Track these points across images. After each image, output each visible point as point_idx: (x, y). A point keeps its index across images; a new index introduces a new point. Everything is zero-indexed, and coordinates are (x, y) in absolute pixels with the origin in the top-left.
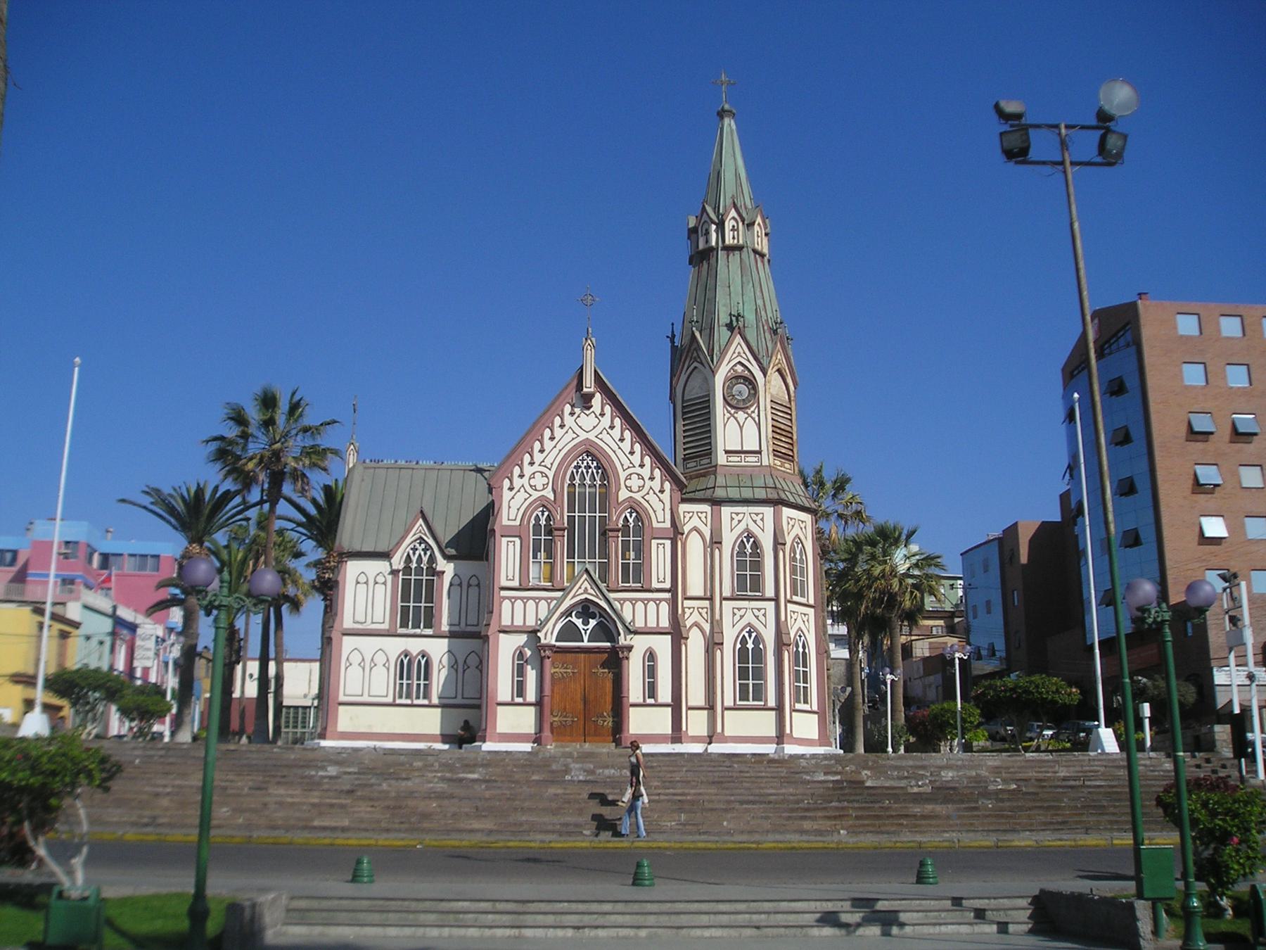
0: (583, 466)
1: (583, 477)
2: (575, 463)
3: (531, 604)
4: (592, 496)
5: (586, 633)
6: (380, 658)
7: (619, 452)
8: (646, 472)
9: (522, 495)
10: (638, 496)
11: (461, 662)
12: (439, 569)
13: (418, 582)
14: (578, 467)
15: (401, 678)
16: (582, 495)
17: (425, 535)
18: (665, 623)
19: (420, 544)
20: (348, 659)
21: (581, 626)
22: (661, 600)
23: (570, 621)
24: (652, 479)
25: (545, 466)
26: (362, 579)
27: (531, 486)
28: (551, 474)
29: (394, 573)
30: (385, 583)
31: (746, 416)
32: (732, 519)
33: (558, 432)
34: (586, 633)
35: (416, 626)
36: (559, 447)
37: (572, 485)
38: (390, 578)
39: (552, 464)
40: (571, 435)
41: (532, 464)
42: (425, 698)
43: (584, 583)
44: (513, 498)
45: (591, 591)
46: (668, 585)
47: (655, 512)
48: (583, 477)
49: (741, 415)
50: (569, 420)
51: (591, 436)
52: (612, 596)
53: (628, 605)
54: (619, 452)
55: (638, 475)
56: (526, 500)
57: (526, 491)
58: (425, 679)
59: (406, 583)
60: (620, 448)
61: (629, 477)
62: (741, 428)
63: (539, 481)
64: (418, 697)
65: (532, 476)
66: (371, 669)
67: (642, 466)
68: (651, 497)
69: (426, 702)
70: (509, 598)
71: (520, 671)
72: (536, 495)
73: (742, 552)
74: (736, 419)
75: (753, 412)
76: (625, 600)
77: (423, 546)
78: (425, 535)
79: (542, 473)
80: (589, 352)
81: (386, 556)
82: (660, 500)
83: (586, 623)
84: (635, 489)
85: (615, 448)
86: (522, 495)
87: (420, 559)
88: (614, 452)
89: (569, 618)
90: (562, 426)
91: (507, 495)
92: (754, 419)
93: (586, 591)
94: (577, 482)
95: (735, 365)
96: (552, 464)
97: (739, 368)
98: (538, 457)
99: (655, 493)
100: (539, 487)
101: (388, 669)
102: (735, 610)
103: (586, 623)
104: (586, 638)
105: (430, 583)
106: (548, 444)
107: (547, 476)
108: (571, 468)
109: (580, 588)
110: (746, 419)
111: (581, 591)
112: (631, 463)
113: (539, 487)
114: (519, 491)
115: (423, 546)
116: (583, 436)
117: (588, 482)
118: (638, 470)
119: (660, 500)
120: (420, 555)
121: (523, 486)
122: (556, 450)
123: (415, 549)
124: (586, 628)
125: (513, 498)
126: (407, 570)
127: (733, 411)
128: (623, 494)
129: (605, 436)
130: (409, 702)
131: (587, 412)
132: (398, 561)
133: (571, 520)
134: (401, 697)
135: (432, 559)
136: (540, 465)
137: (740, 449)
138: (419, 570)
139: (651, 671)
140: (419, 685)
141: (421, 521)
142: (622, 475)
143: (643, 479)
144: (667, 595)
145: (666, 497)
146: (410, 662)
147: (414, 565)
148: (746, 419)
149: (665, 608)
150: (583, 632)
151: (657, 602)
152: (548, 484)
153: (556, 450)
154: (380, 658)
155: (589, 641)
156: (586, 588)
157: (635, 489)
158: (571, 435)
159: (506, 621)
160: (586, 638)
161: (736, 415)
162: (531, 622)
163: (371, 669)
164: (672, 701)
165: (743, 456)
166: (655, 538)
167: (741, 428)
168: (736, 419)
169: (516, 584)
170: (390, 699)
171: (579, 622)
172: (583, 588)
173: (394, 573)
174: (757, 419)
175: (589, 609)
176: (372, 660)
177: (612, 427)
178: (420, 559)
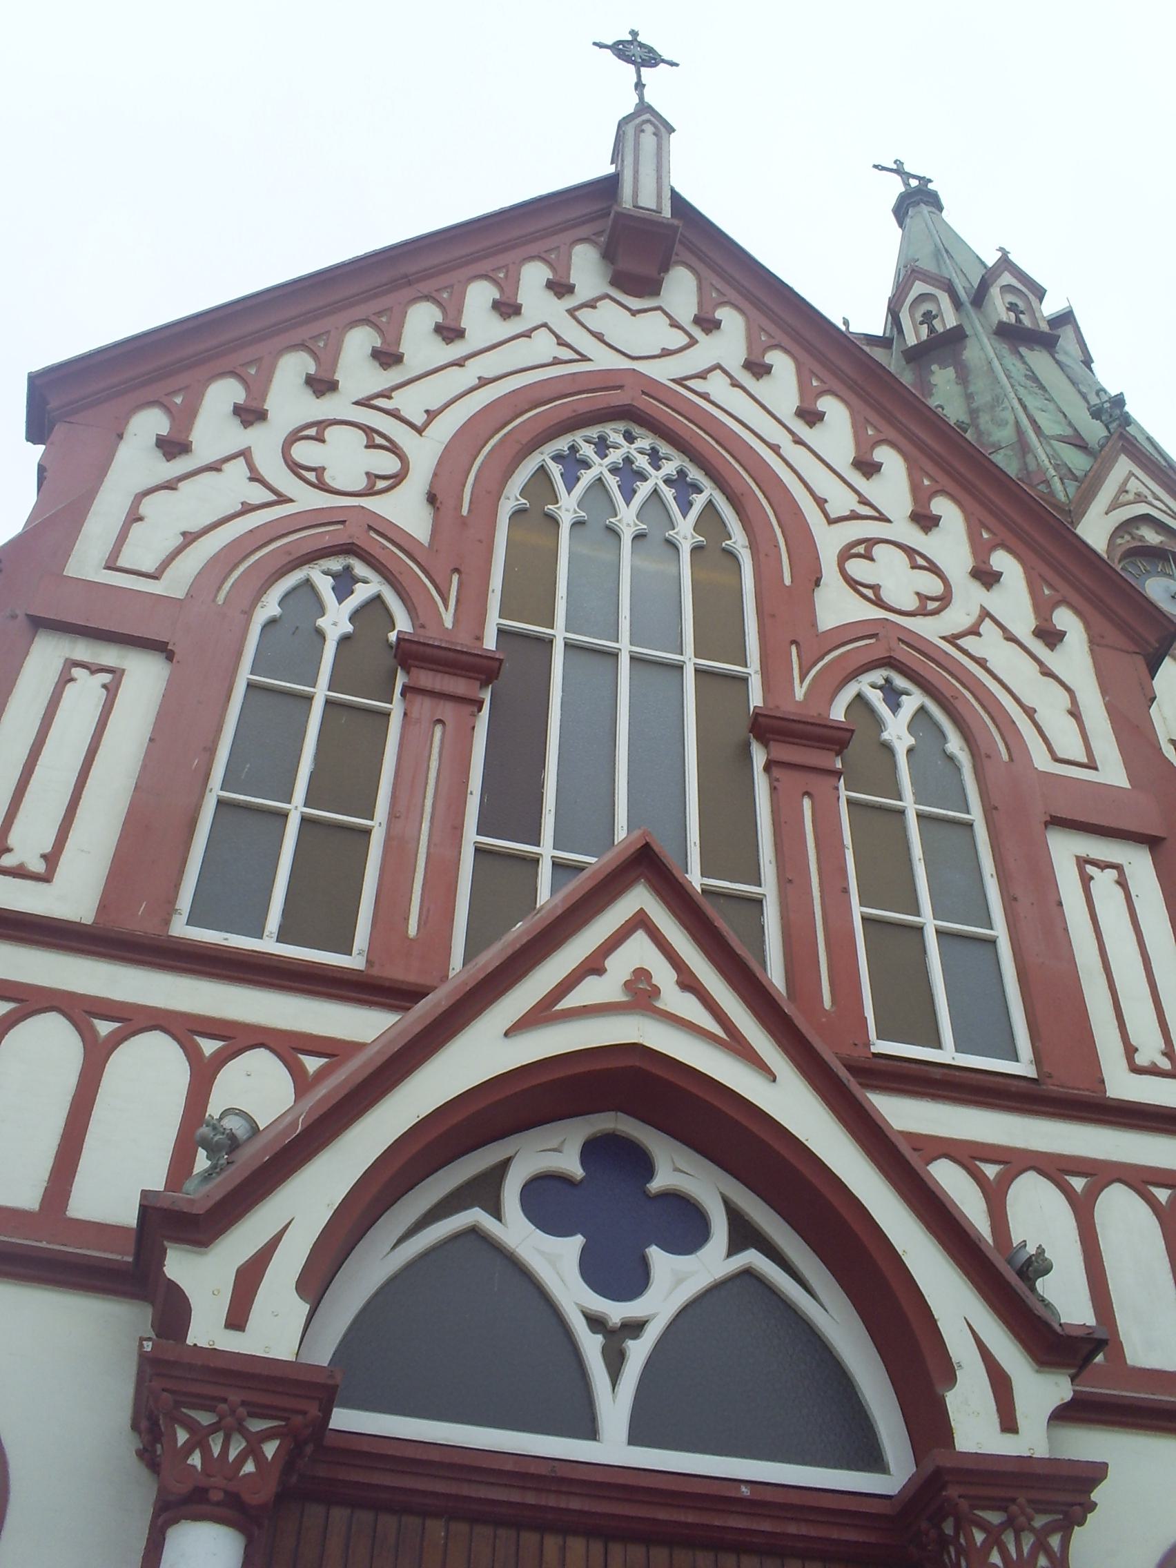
0: (626, 448)
5: (615, 1361)
23: (474, 1231)
25: (395, 414)
34: (615, 1361)
45: (675, 1000)
47: (1030, 712)
56: (247, 509)
60: (798, 441)
61: (865, 549)
79: (368, 431)
82: (1047, 673)
88: (775, 449)
89: (475, 1216)
99: (1010, 638)
109: (593, 966)
112: (864, 501)
114: (215, 467)
124: (616, 1312)
125: (170, 486)
136: (364, 403)
150: (591, 1345)
155: (636, 1437)
172: (620, 965)
175: (646, 1167)
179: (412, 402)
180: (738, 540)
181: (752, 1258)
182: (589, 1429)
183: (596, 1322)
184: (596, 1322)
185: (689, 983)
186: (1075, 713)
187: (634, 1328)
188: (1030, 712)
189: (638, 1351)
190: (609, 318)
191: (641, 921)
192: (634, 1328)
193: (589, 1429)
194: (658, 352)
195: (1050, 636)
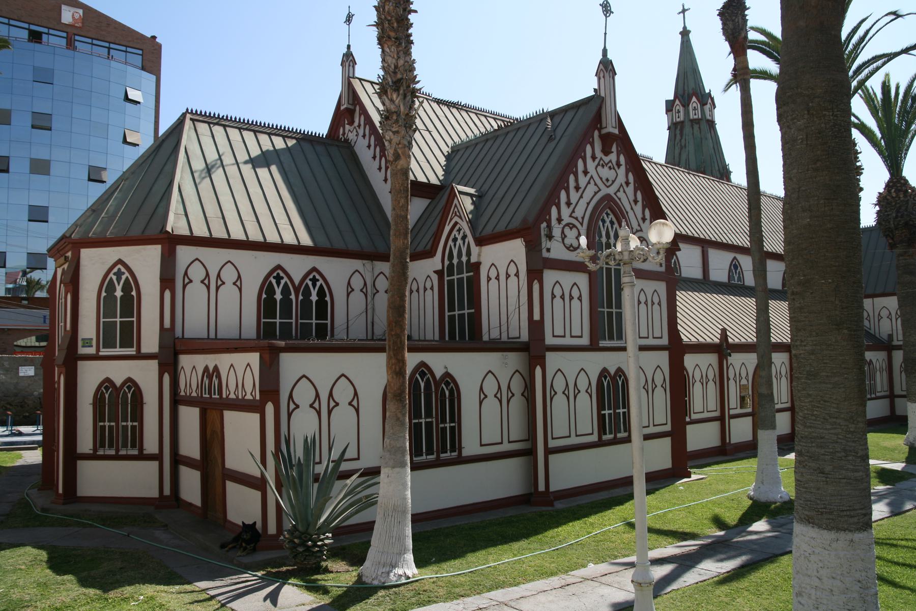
25: (576, 219)
33: (583, 180)
50: (591, 165)
51: (611, 191)
90: (586, 172)
116: (605, 191)
129: (621, 194)
131: (606, 159)
177: (627, 183)
179: (579, 213)
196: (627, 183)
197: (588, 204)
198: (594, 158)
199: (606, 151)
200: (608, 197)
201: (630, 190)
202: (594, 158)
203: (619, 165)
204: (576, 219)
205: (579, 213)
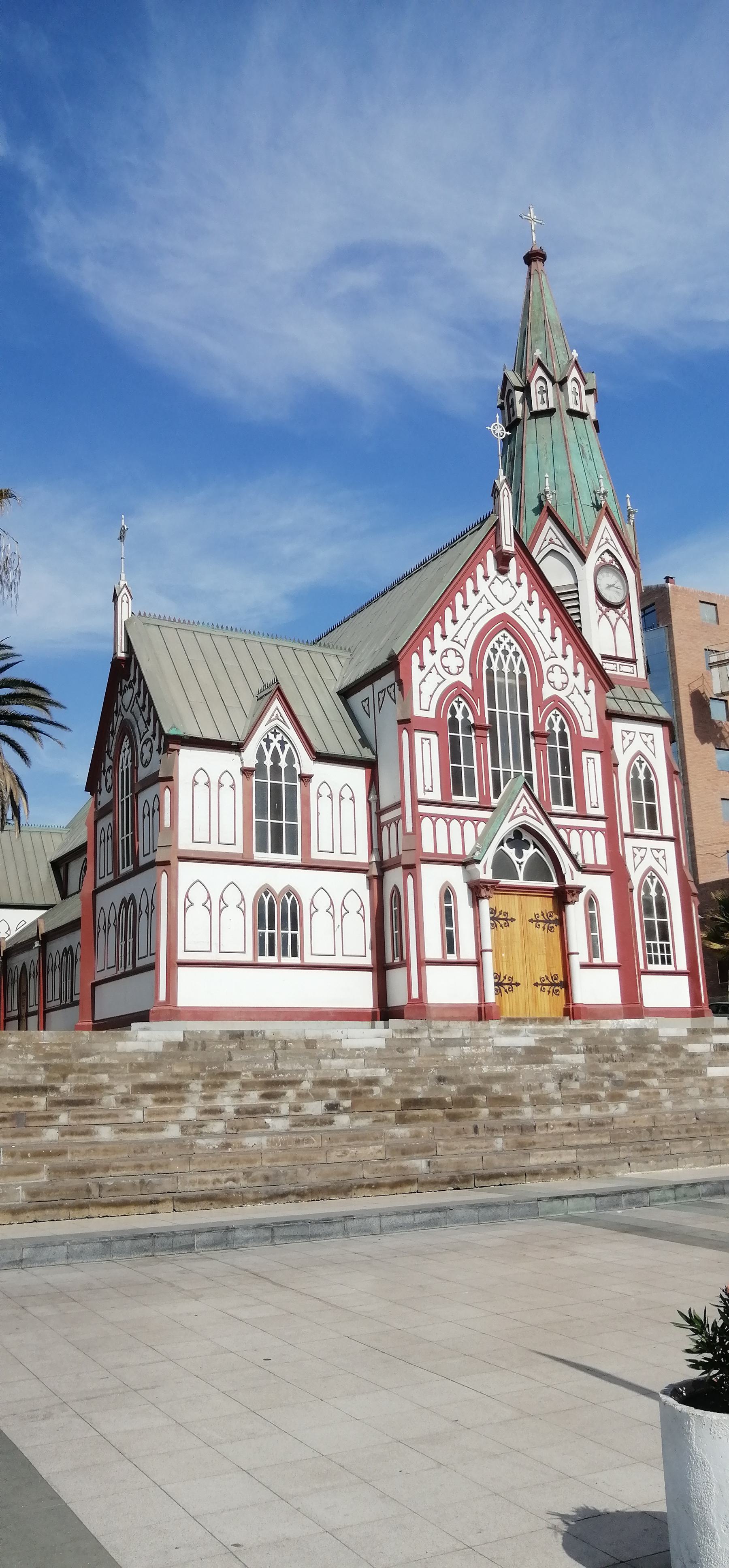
1: (500, 664)
2: (490, 646)
3: (469, 825)
4: (512, 687)
5: (520, 867)
6: (233, 898)
7: (538, 635)
8: (568, 664)
9: (433, 679)
10: (562, 695)
11: (338, 906)
12: (305, 772)
13: (276, 789)
14: (494, 651)
15: (262, 926)
16: (502, 686)
17: (284, 722)
18: (603, 860)
19: (275, 734)
20: (187, 896)
21: (515, 859)
22: (597, 830)
23: (501, 849)
24: (576, 674)
25: (458, 642)
26: (201, 778)
27: (444, 667)
28: (467, 654)
29: (246, 772)
30: (233, 786)
31: (617, 616)
32: (623, 738)
33: (472, 599)
34: (520, 867)
35: (277, 849)
36: (474, 618)
37: (490, 673)
38: (239, 778)
39: (466, 641)
40: (484, 606)
41: (444, 636)
42: (294, 954)
43: (523, 802)
44: (424, 680)
45: (530, 812)
46: (601, 812)
47: (581, 717)
48: (500, 664)
49: (612, 614)
50: (482, 585)
51: (508, 610)
52: (555, 821)
53: (574, 834)
54: (538, 635)
55: (561, 667)
56: (439, 684)
57: (438, 674)
58: (294, 928)
59: (261, 787)
62: (614, 629)
63: (452, 662)
64: (285, 954)
65: (444, 655)
66: (221, 911)
67: (565, 656)
68: (575, 697)
69: (296, 961)
70: (430, 816)
71: (448, 916)
72: (451, 680)
73: (636, 781)
74: (608, 618)
75: (624, 612)
76: (572, 828)
77: (279, 737)
78: (284, 722)
79: (455, 650)
80: (506, 498)
81: (237, 748)
83: (520, 855)
84: (559, 686)
85: (535, 630)
86: (433, 679)
87: (275, 757)
90: (476, 592)
91: (417, 675)
92: (625, 621)
93: (525, 812)
94: (495, 668)
95: (603, 554)
96: (466, 641)
97: (607, 558)
98: (450, 629)
99: (579, 694)
100: (454, 670)
101: (244, 913)
102: (635, 850)
103: (520, 855)
104: (521, 874)
105: (292, 790)
106: (461, 613)
107: (461, 656)
108: (488, 651)
110: (618, 619)
111: (519, 811)
113: (454, 670)
115: (279, 737)
116: (499, 610)
117: (506, 669)
118: (560, 661)
119: (586, 704)
120: (275, 748)
121: (434, 665)
122: (469, 624)
123: (268, 741)
124: (520, 861)
125: (424, 680)
126: (259, 770)
127: (604, 608)
128: (547, 692)
129: (521, 612)
130: (273, 960)
131: (503, 578)
132: (249, 758)
133: (492, 715)
134: (262, 953)
135: (290, 759)
136: (452, 640)
137: (613, 654)
138: (276, 770)
139: (592, 922)
140: (285, 937)
141: (276, 703)
142: (545, 666)
143: (566, 673)
144: (602, 824)
145: (591, 698)
146: (271, 904)
147: (268, 763)
148: (618, 619)
149: (600, 838)
150: (517, 866)
151: (593, 830)
152: (463, 666)
153: (469, 624)
154: (233, 898)
156: (525, 807)
157: (559, 686)
158: (484, 606)
159: (428, 847)
160: (521, 874)
161: (607, 613)
162: (457, 850)
163: (221, 911)
164: (619, 961)
165: (618, 663)
166: (585, 750)
167: (614, 629)
168: (608, 618)
169: (436, 796)
170: (248, 958)
171: (511, 852)
173: (246, 772)
174: (628, 621)
175: (522, 837)
176: (222, 898)
177: (530, 602)
178: (275, 757)
179: (461, 638)
180: (527, 672)
181: (536, 850)
182: (517, 878)
183: (518, 863)
184: (518, 863)
185: (531, 808)
186: (590, 715)
187: (522, 863)
188: (581, 717)
189: (523, 866)
190: (497, 587)
191: (524, 796)
192: (522, 863)
193: (517, 878)
194: (508, 600)
195: (587, 692)
196: (530, 602)
197: (475, 624)
198: (486, 577)
199: (503, 570)
200: (504, 617)
201: (535, 609)
202: (486, 577)
203: (519, 584)
204: (458, 642)
205: (461, 638)
